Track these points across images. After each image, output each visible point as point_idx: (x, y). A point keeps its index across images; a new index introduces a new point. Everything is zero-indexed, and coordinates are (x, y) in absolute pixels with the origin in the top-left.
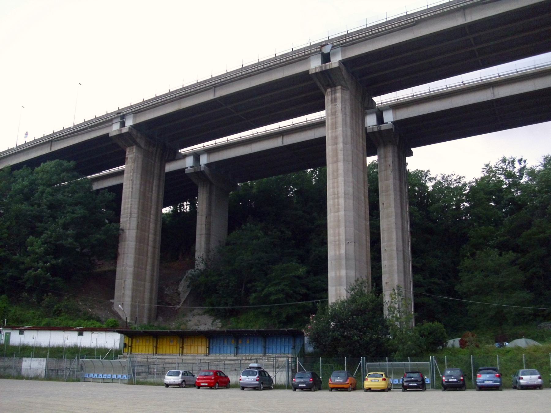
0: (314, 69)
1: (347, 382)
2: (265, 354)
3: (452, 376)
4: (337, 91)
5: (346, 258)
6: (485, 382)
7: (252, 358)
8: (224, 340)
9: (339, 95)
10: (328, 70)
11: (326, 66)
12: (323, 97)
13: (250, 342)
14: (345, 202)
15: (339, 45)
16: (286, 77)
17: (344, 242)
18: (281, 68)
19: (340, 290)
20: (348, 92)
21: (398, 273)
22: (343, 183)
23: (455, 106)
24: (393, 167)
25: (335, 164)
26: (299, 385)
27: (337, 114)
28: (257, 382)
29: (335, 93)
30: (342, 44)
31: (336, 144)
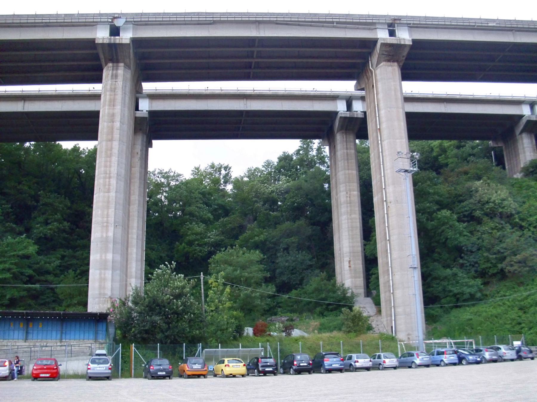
0: (101, 39)
1: (204, 369)
2: (61, 339)
3: (303, 360)
4: (119, 68)
5: (114, 242)
6: (333, 365)
7: (48, 345)
8: (19, 324)
9: (121, 71)
10: (117, 44)
11: (115, 39)
12: (102, 70)
13: (42, 326)
14: (117, 183)
15: (131, 21)
16: (66, 39)
17: (113, 225)
18: (60, 28)
19: (105, 274)
20: (129, 71)
21: (137, 261)
22: (116, 163)
23: (209, 109)
24: (141, 156)
25: (109, 143)
26: (159, 373)
27: (116, 91)
28: (110, 371)
29: (117, 69)
30: (134, 22)
31: (113, 122)
